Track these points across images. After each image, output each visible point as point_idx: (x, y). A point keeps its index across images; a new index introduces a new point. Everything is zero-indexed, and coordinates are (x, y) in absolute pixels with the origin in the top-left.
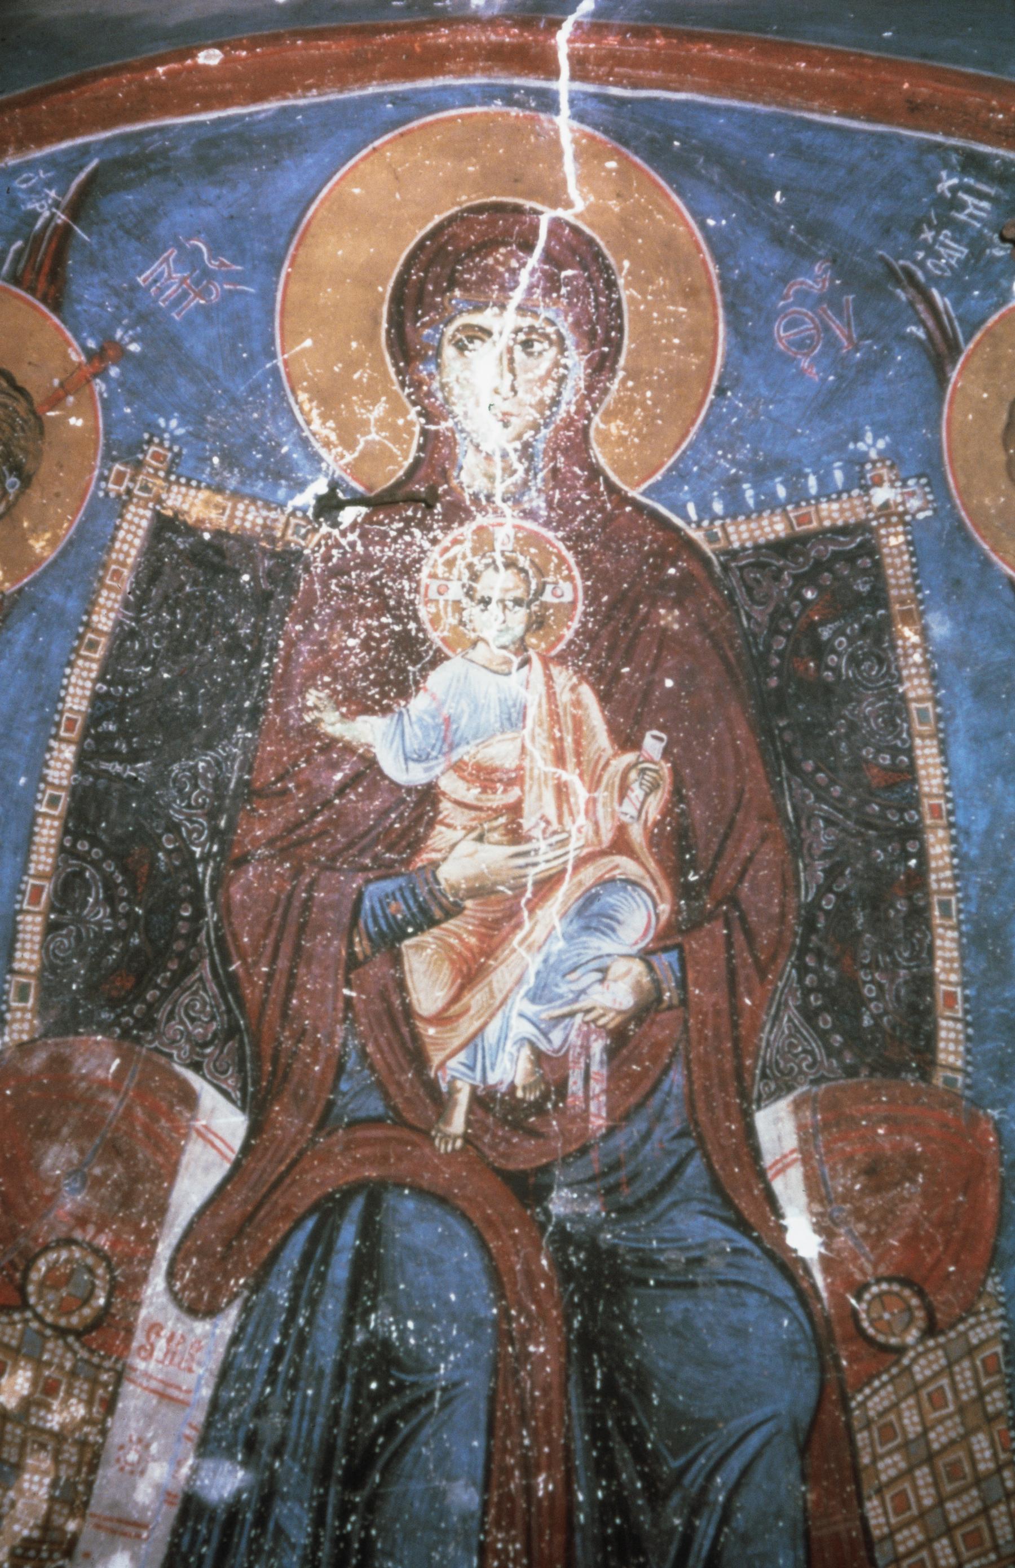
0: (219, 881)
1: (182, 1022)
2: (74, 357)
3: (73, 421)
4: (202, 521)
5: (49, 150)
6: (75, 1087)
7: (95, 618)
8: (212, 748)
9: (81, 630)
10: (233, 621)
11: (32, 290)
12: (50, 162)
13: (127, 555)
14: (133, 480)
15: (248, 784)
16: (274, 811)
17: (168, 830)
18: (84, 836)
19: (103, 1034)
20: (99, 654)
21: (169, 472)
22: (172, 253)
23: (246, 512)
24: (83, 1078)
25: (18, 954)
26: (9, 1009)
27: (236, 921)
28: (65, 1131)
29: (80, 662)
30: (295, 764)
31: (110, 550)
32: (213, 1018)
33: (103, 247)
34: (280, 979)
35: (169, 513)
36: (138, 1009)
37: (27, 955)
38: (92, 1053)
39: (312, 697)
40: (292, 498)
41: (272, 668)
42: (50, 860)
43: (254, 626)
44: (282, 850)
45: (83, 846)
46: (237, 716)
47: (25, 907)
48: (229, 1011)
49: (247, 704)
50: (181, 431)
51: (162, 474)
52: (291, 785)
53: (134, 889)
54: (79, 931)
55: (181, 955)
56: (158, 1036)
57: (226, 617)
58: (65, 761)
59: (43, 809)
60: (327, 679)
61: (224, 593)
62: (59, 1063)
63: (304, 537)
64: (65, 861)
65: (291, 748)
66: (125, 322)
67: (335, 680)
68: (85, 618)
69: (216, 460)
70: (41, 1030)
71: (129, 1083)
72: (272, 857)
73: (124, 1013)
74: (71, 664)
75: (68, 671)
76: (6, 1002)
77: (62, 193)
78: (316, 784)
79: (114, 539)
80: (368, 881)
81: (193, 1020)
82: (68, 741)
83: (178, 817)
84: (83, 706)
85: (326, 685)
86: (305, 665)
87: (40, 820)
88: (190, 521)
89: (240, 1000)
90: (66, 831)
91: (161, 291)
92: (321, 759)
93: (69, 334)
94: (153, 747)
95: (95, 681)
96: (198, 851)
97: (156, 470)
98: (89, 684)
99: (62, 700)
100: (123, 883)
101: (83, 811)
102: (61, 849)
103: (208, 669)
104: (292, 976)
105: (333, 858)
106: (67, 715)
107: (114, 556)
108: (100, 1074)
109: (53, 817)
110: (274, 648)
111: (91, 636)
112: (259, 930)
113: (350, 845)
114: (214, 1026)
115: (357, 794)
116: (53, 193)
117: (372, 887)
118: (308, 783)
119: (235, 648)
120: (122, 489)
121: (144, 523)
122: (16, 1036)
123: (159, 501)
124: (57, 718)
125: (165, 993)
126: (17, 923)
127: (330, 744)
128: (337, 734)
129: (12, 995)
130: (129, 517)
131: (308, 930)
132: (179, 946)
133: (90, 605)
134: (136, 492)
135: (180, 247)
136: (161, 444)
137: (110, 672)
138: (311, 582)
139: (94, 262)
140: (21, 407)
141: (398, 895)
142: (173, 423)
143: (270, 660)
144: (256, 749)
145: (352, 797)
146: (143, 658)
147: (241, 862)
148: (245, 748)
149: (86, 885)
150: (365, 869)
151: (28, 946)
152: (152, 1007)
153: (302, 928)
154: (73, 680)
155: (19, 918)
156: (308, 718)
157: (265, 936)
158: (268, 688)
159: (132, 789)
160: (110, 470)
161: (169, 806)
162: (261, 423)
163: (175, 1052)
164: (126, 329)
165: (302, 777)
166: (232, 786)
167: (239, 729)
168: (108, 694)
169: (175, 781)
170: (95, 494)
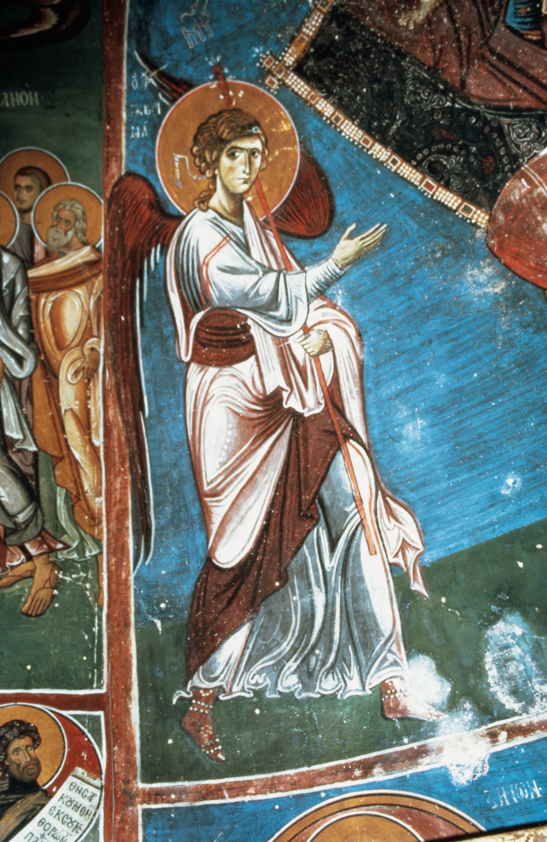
0: (466, 99)
1: (523, 142)
2: (214, 86)
3: (240, 95)
4: (304, 50)
5: (125, 71)
6: (522, 205)
7: (326, 114)
8: (406, 79)
9: (328, 122)
10: (353, 50)
11: (180, 95)
12: (130, 72)
13: (306, 90)
14: (274, 76)
15: (429, 68)
16: (448, 59)
17: (432, 115)
18: (416, 154)
19: (507, 181)
20: (342, 117)
21: (277, 59)
22: (184, 30)
23: (307, 28)
24: (521, 199)
25: (450, 205)
26: (471, 219)
27: (488, 96)
28: (539, 218)
29: (342, 127)
30: (431, 41)
31: (300, 97)
32: (530, 126)
33: (172, 60)
34: (530, 84)
35: (295, 64)
36: (505, 160)
37: (452, 201)
38: (512, 190)
39: (402, 22)
40: (308, 3)
41: (382, 38)
42: (418, 174)
43: (360, 40)
44: (468, 62)
45: (420, 156)
46: (397, 62)
47: (431, 193)
48: (531, 116)
49: (393, 56)
50: (262, 48)
51: (277, 63)
52: (440, 46)
53: (450, 141)
54: (456, 174)
55: (492, 130)
56: (523, 157)
57: (350, 53)
58: (380, 150)
59: (394, 168)
60: (396, 12)
61: (340, 50)
62: (508, 207)
63: (327, 3)
64: (422, 167)
65: (422, 41)
66: (206, 59)
67: (398, 8)
68: (324, 118)
69: (279, 36)
70: (488, 209)
71: (537, 178)
72: (468, 68)
73: (503, 168)
74: (341, 131)
75: (343, 134)
76: (467, 219)
77: (144, 70)
78: (444, 33)
79: (296, 94)
80: (504, 21)
81: (525, 136)
82: (373, 145)
83: (429, 108)
84: (361, 132)
85: (399, 13)
86: (386, 20)
87: (399, 171)
88: (303, 56)
89: (529, 109)
90: (409, 162)
91: (198, 39)
92: (433, 27)
93: (204, 85)
94: (392, 108)
95: (353, 123)
96: (448, 104)
97: (274, 64)
98: (353, 127)
99: (354, 141)
100: (445, 145)
101: (405, 152)
102: (415, 167)
103: (371, 69)
104: (532, 78)
105: (484, 36)
106: (361, 142)
107: (304, 96)
108: (523, 191)
109: (401, 165)
110: (374, 34)
111: (333, 119)
112: (500, 87)
113: (482, 24)
114: (534, 127)
115: (458, 13)
116: (144, 75)
117: (508, 20)
118: (442, 38)
119: (366, 53)
120: (277, 82)
121: (295, 77)
122: (484, 221)
123: (288, 68)
124: (360, 147)
125: (506, 145)
126: (436, 201)
127: (428, 20)
128: (425, 14)
129: (466, 215)
130: (290, 83)
131: (513, 61)
132: (487, 130)
133: (320, 114)
134: (280, 77)
135: (182, 25)
136: (264, 59)
137: (351, 115)
138: (349, 6)
139: (177, 66)
140: (226, 115)
141: (518, 6)
142: (257, 50)
143: (378, 38)
144: (416, 58)
145: (459, 16)
146: (352, 99)
147: (463, 84)
148: (413, 64)
149: (437, 162)
150: (497, 21)
151: (449, 199)
152: (508, 153)
153: (511, 64)
154: (348, 133)
155: (435, 198)
156: (412, 27)
157: (504, 84)
158: (390, 43)
159: (406, 124)
160: (266, 85)
161: (422, 110)
162: (270, 9)
163: (535, 151)
164: (210, 60)
165: (438, 39)
166: (426, 76)
167: (403, 63)
168: (361, 120)
169: (412, 103)
170: (276, 96)
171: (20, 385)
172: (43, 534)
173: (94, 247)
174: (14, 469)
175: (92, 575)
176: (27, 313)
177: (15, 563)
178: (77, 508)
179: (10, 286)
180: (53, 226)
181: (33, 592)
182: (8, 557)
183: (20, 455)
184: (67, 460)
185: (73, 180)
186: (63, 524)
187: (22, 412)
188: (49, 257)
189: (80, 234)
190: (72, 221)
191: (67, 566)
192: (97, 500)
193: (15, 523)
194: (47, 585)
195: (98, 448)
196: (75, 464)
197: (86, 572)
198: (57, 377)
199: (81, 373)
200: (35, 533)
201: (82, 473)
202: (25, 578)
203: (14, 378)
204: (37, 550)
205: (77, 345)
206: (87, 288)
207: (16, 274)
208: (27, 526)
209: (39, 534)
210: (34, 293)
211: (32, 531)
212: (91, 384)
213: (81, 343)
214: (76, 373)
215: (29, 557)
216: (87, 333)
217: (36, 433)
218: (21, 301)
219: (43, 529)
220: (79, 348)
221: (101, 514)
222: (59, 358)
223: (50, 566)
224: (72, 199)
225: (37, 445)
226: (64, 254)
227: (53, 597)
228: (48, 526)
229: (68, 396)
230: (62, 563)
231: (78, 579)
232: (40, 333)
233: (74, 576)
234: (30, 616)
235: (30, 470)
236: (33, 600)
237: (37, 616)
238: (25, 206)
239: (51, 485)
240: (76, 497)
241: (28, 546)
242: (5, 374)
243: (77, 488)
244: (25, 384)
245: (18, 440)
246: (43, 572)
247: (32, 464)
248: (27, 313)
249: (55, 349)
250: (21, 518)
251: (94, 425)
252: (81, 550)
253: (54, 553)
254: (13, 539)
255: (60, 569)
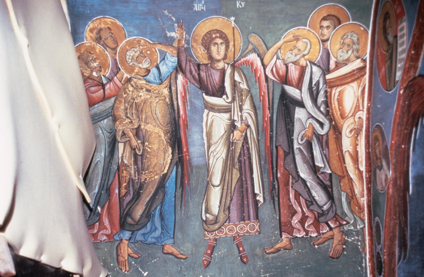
171: (322, 138)
172: (336, 216)
173: (362, 59)
174: (320, 183)
175: (361, 238)
176: (325, 99)
177: (324, 231)
178: (352, 203)
179: (317, 85)
180: (340, 49)
181: (334, 246)
182: (321, 228)
183: (323, 175)
184: (346, 178)
185: (353, 20)
186: (346, 211)
187: (323, 153)
188: (338, 66)
189: (355, 52)
190: (351, 44)
191: (348, 233)
192: (362, 199)
193: (322, 211)
194: (340, 243)
195: (362, 172)
196: (350, 180)
197: (358, 237)
198: (341, 134)
199: (354, 131)
200: (333, 216)
201: (354, 185)
202: (329, 239)
203: (319, 134)
204: (334, 225)
205: (352, 116)
206: (357, 83)
207: (320, 78)
208: (328, 212)
209: (334, 217)
210: (329, 88)
211: (331, 215)
212: (359, 138)
213: (354, 115)
214: (351, 131)
215: (331, 229)
216: (357, 109)
217: (331, 163)
218: (322, 93)
219: (336, 214)
220: (353, 117)
221: (364, 207)
222: (342, 123)
223: (341, 233)
224: (352, 32)
225: (331, 170)
226: (346, 64)
227: (344, 249)
228: (339, 212)
229: (347, 144)
230: (346, 231)
231: (354, 240)
232: (332, 110)
233: (352, 239)
234: (333, 258)
235: (328, 183)
236: (334, 250)
237: (337, 258)
238: (325, 38)
239: (339, 191)
240: (351, 197)
241: (329, 223)
242: (314, 133)
243: (352, 192)
244: (325, 137)
245: (321, 167)
246: (337, 236)
247: (329, 180)
248: (325, 99)
249: (340, 118)
250: (325, 208)
251: (360, 160)
252: (355, 227)
253: (342, 227)
254: (322, 219)
255: (346, 235)
